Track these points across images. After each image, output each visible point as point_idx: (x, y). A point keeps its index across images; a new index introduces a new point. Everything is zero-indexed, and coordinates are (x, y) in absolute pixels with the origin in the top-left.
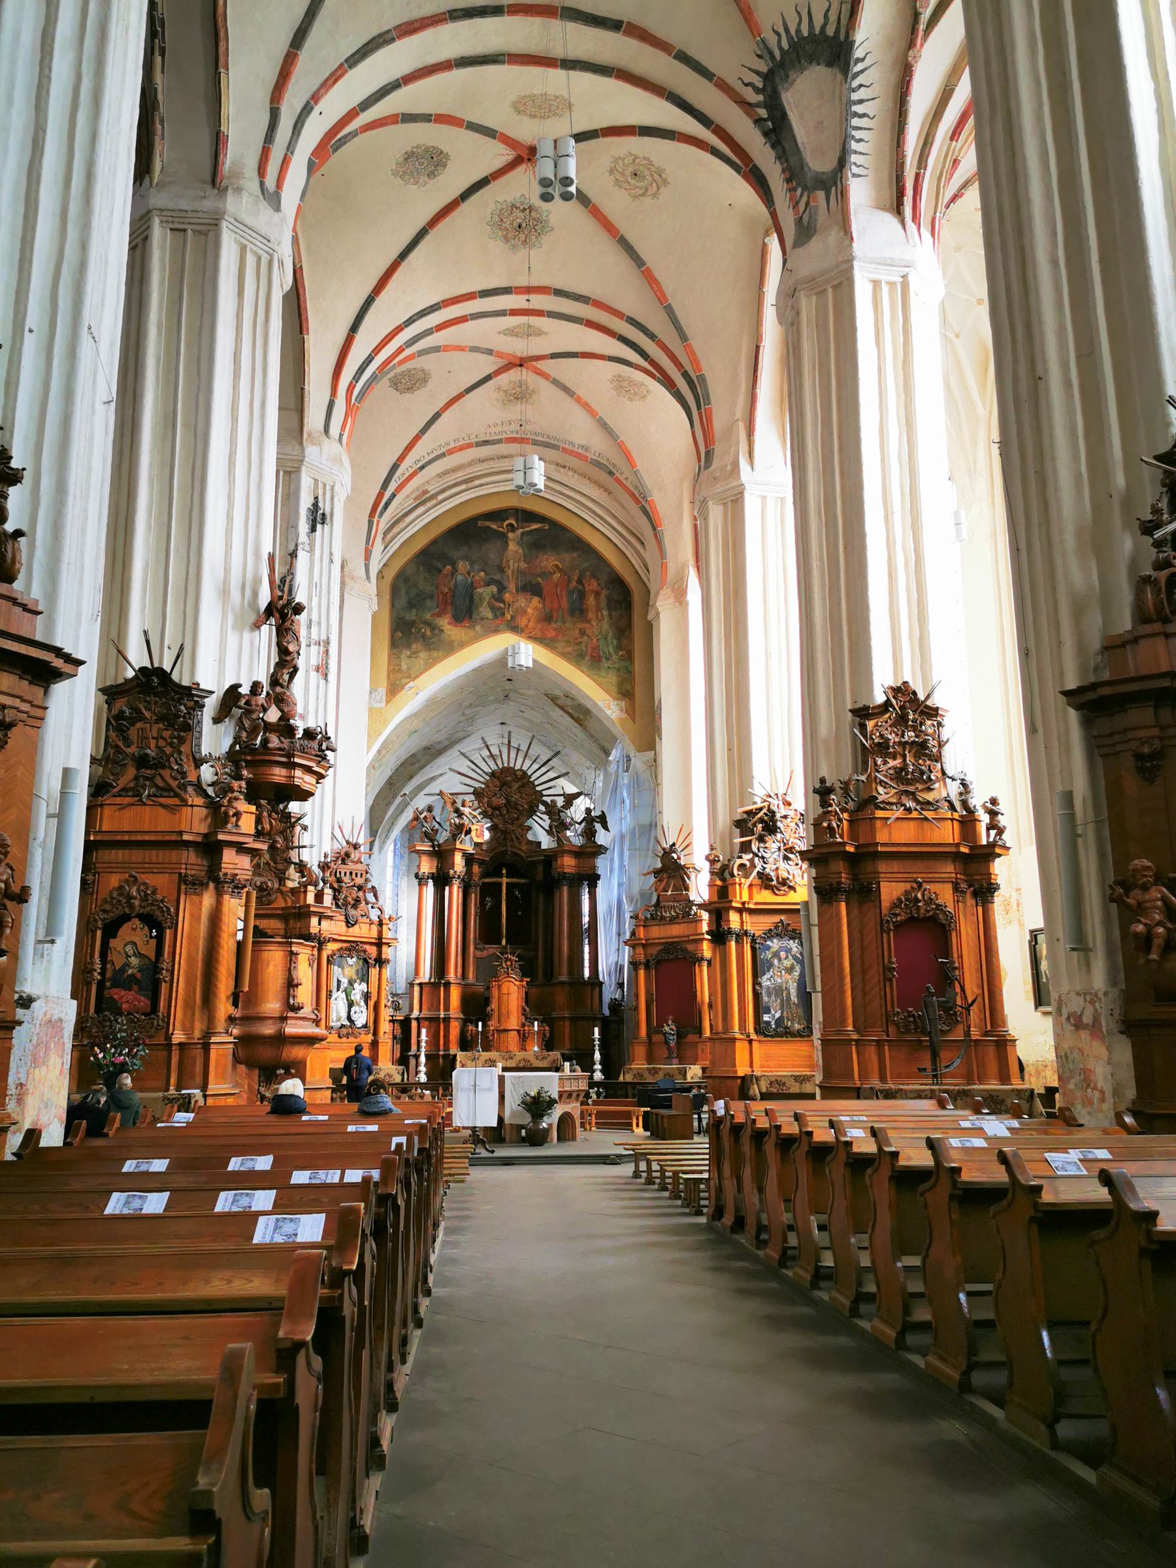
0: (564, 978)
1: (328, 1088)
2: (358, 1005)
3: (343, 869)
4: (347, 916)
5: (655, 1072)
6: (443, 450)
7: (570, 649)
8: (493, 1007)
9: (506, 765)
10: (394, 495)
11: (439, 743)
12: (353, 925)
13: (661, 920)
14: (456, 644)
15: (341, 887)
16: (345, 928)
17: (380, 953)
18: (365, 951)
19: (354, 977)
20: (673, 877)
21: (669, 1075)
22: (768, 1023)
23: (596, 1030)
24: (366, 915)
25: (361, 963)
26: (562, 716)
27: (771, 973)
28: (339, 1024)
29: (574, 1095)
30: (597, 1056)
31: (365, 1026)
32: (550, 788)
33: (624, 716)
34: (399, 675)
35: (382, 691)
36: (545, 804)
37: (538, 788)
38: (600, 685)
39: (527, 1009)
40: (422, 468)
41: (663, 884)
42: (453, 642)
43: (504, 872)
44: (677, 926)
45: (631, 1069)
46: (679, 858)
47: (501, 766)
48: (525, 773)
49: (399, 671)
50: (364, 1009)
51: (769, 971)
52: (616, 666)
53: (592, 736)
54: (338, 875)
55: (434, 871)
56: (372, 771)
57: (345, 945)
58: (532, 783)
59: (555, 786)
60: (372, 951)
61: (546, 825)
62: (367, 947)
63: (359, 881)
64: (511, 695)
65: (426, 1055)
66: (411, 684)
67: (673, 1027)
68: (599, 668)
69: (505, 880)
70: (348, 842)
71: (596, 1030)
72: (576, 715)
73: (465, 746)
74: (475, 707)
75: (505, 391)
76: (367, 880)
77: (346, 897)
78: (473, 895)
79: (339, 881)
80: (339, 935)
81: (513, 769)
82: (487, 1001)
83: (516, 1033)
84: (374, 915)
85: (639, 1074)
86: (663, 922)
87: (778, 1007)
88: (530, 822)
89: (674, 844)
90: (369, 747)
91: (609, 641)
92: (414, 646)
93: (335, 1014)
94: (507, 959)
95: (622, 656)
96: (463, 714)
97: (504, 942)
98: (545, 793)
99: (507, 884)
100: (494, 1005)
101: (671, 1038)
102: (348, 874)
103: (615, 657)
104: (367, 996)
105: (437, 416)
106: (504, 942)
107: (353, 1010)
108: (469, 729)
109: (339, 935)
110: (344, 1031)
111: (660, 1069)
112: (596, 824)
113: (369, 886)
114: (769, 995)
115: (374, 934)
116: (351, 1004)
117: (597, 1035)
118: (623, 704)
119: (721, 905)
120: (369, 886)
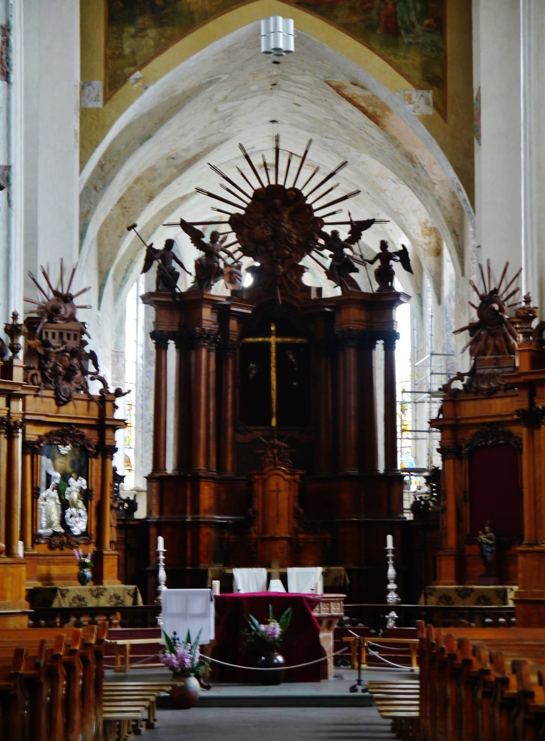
0: (353, 471)
1: (24, 613)
2: (75, 506)
3: (52, 329)
4: (57, 391)
5: (464, 594)
7: (355, 19)
8: (256, 507)
9: (273, 182)
11: (187, 150)
12: (65, 403)
13: (476, 393)
14: (197, 16)
15: (48, 353)
16: (54, 407)
17: (102, 437)
18: (82, 436)
19: (69, 470)
20: (494, 335)
21: (483, 598)
23: (390, 538)
24: (85, 388)
25: (77, 452)
26: (351, 111)
28: (50, 531)
29: (325, 622)
30: (391, 572)
31: (84, 534)
32: (334, 213)
33: (430, 111)
34: (120, 62)
35: (98, 85)
36: (324, 236)
37: (317, 214)
38: (398, 69)
39: (301, 510)
41: (481, 344)
42: (192, 13)
43: (273, 328)
44: (498, 402)
45: (434, 590)
46: (501, 309)
47: (266, 184)
48: (298, 193)
49: (121, 56)
50: (83, 512)
52: (420, 40)
53: (392, 139)
54: (44, 337)
55: (175, 329)
56: (94, 192)
57: (56, 429)
58: (310, 206)
59: (340, 211)
60: (92, 436)
61: (328, 263)
62: (85, 431)
63: (72, 344)
64: (282, 83)
65: (166, 570)
66: (138, 74)
67: (491, 535)
68: (396, 46)
69: (273, 340)
70: (56, 293)
71: (390, 538)
72: (370, 109)
73: (214, 158)
74: (231, 100)
76: (85, 343)
77: (55, 365)
78: (230, 361)
79: (46, 344)
80: (47, 416)
81: (283, 187)
82: (249, 499)
83: (285, 542)
84: (95, 388)
85: (445, 597)
86: (480, 396)
88: (306, 261)
89: (496, 291)
90: (83, 163)
91: (411, 5)
92: (140, 21)
94: (273, 446)
95: (429, 26)
96: (216, 111)
97: (274, 422)
98: (326, 220)
99: (278, 344)
100: (257, 505)
101: (489, 549)
102: (57, 335)
103: (419, 29)
104: (86, 495)
106: (274, 422)
107: (69, 512)
108: (227, 130)
109: (47, 416)
110: (57, 541)
111: (472, 590)
112: (392, 262)
113: (87, 349)
115: (95, 413)
116: (65, 505)
117: (390, 545)
118: (430, 95)
119: (533, 377)
120: (87, 349)
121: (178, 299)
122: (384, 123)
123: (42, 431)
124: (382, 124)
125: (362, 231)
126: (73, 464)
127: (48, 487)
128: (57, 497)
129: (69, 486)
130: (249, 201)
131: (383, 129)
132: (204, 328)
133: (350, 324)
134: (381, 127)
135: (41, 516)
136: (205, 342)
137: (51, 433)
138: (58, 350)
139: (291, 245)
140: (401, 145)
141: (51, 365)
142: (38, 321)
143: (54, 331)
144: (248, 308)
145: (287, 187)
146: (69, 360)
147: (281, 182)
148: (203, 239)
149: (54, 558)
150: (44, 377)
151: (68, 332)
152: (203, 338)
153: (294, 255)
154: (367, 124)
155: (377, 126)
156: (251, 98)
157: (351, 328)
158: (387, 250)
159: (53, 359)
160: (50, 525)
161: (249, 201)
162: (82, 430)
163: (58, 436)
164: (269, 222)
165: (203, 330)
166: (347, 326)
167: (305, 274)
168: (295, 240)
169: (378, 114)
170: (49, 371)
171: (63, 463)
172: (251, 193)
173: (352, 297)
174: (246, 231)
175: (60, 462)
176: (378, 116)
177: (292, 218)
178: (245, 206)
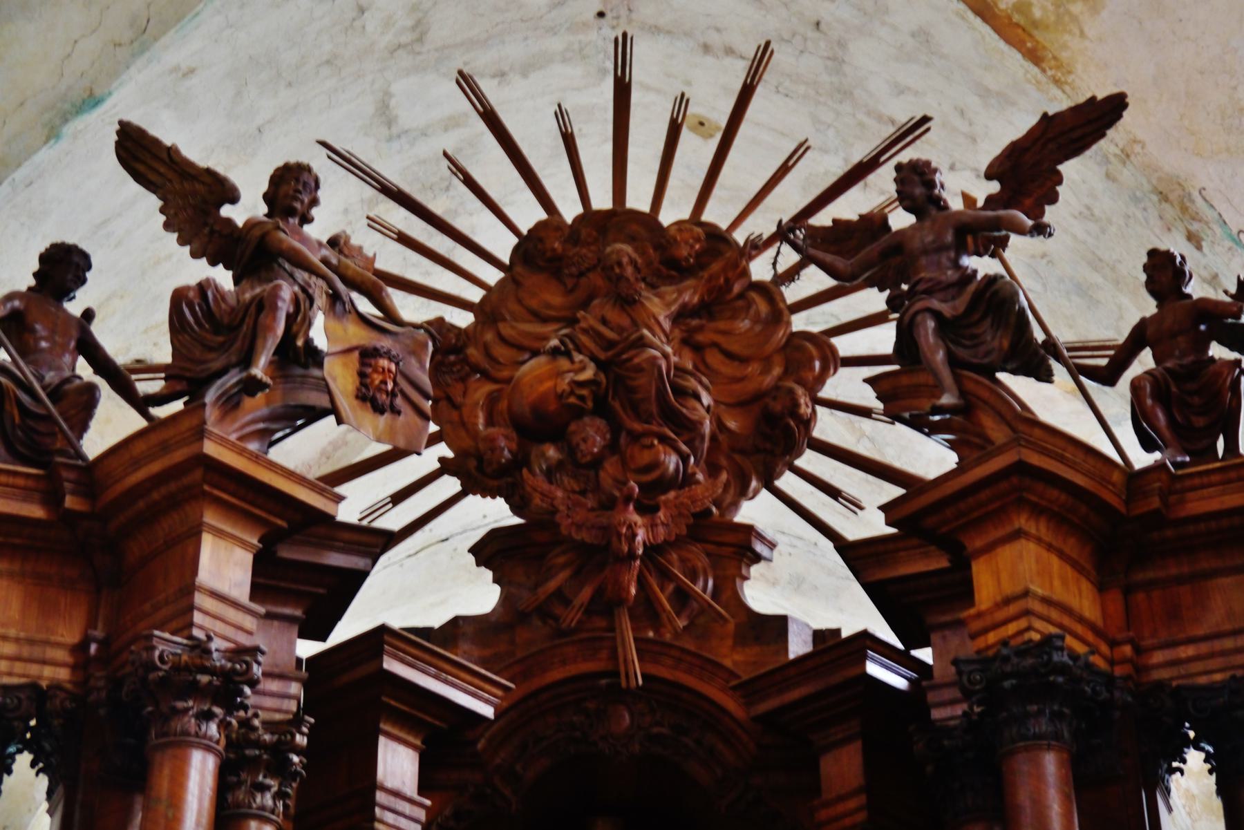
9: (602, 200)
47: (570, 210)
48: (717, 239)
81: (649, 220)
98: (846, 345)
121: (70, 502)
122: (1064, 55)
124: (1055, 58)
125: (1061, 162)
130: (492, 276)
131: (1057, 82)
132: (197, 633)
133: (1027, 613)
134: (1050, 73)
136: (207, 716)
139: (688, 428)
140: (1137, 148)
144: (477, 684)
145: (667, 217)
147: (639, 198)
148: (226, 211)
152: (194, 690)
153: (700, 477)
154: (985, 93)
155: (1035, 70)
156: (526, 70)
157: (1036, 637)
158: (1189, 296)
161: (492, 276)
164: (584, 339)
165: (201, 648)
166: (1012, 628)
167: (755, 570)
168: (708, 409)
169: (1037, 13)
172: (503, 244)
173: (1035, 459)
174: (481, 391)
176: (1035, 24)
177: (688, 342)
178: (475, 295)
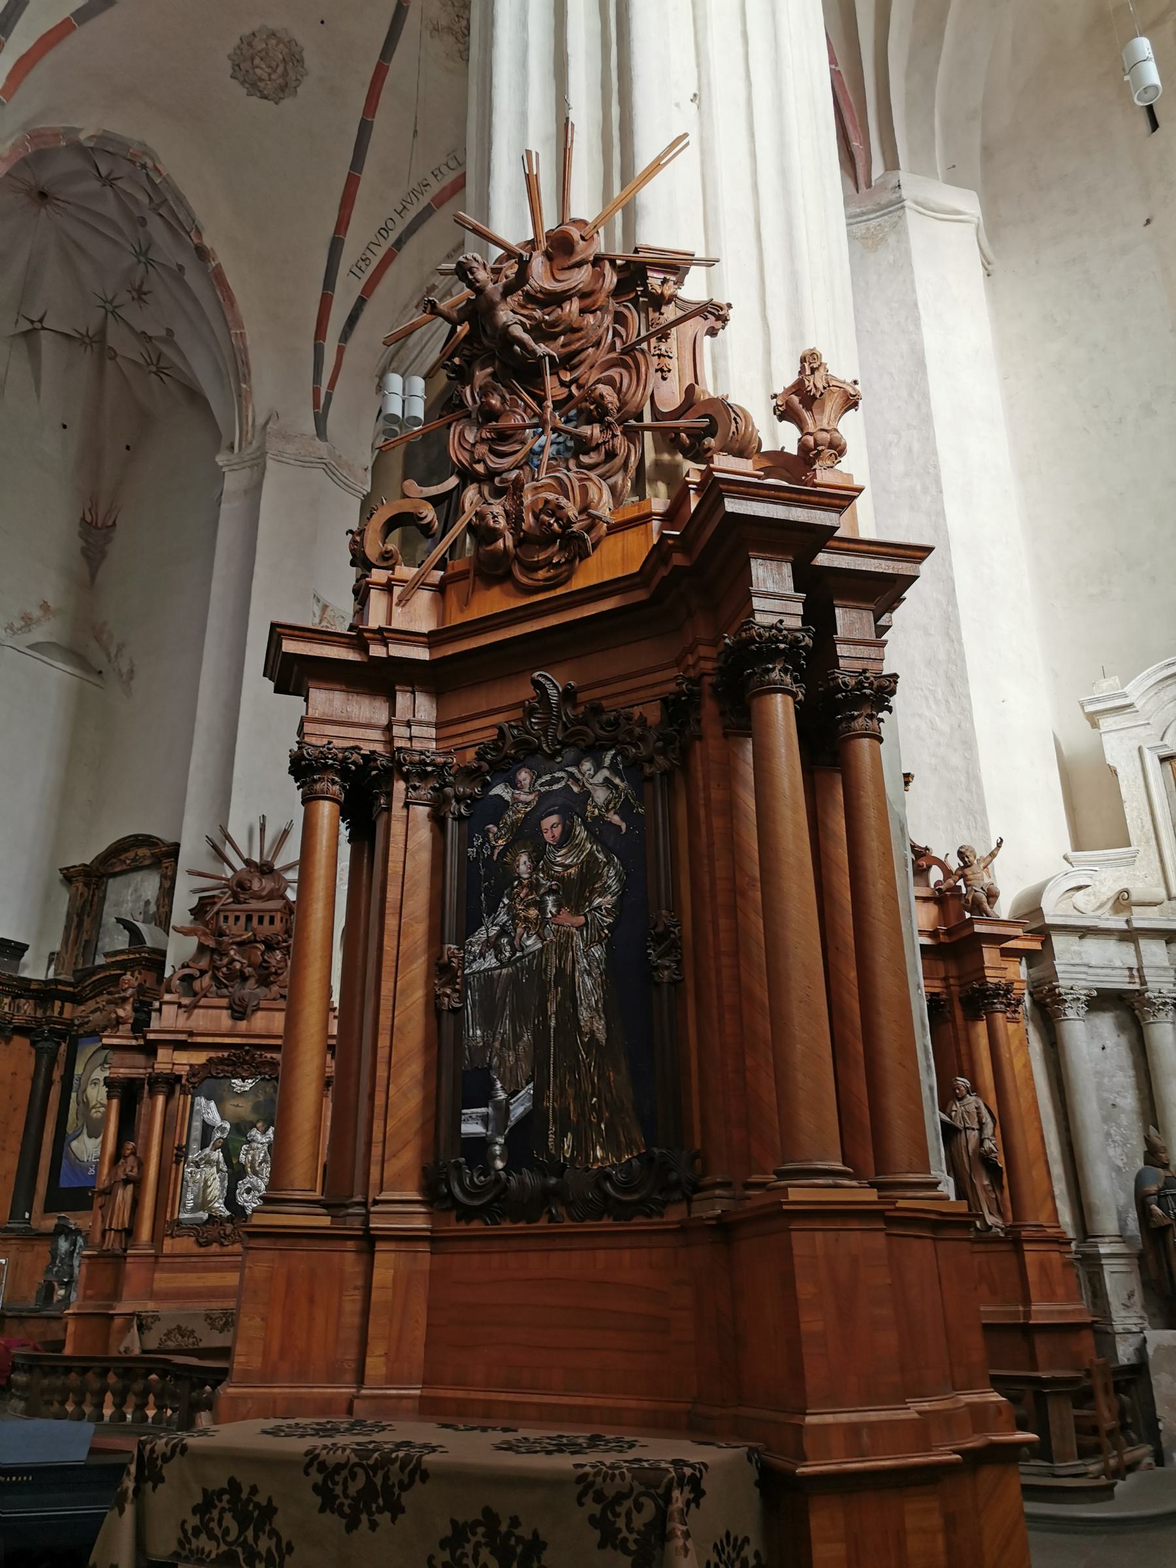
6: (425, 200)
10: (361, 302)
22: (480, 1146)
27: (503, 918)
40: (399, 244)
51: (493, 910)
63: (266, 930)
70: (248, 862)
75: (450, 29)
87: (525, 1068)
93: (190, 1196)
102: (243, 919)
105: (365, 128)
107: (243, 1185)
110: (214, 1231)
114: (489, 1022)
116: (236, 1173)
123: (200, 1058)
126: (256, 1108)
127: (203, 1146)
128: (221, 1159)
129: (249, 1142)
135: (187, 1191)
137: (210, 1060)
138: (238, 939)
141: (225, 960)
142: (211, 901)
143: (237, 914)
146: (263, 954)
149: (206, 1259)
150: (215, 978)
151: (261, 914)
159: (232, 952)
160: (203, 1203)
162: (269, 1055)
163: (228, 1065)
170: (224, 969)
171: (243, 1108)
175: (230, 1105)
